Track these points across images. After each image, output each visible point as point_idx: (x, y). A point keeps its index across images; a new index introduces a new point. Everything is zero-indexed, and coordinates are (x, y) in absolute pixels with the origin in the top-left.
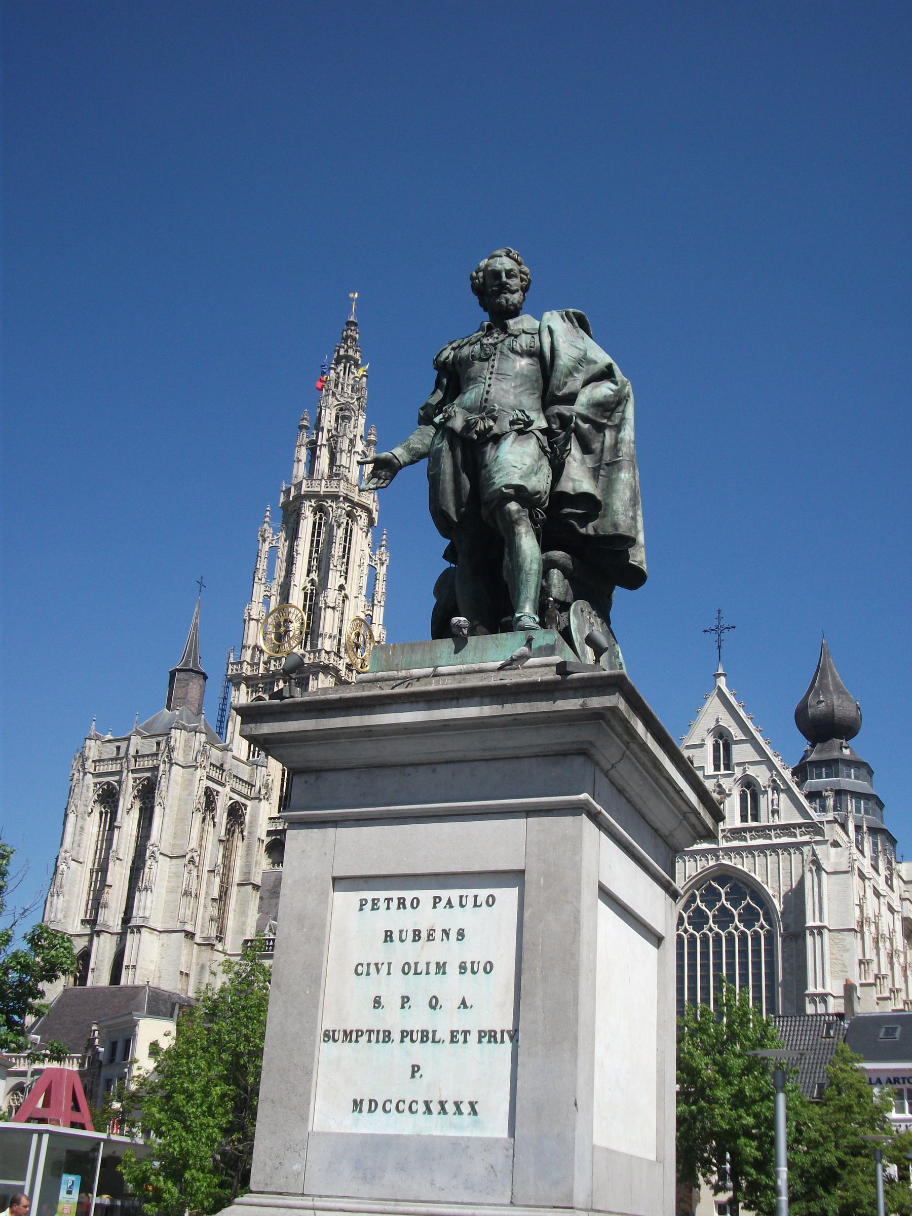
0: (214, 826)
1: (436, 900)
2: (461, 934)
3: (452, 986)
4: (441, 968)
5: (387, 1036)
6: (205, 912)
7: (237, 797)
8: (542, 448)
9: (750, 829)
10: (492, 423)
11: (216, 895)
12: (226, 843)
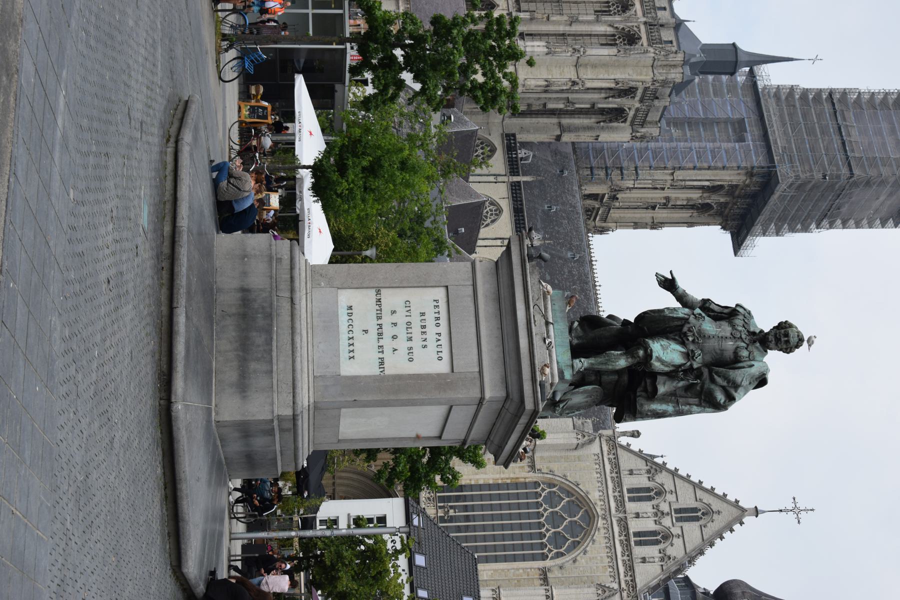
0: (606, 98)
1: (439, 334)
2: (425, 346)
3: (402, 345)
4: (410, 339)
5: (379, 318)
6: (535, 99)
7: (631, 114)
8: (680, 366)
9: (628, 540)
10: (691, 339)
11: (550, 106)
12: (592, 111)
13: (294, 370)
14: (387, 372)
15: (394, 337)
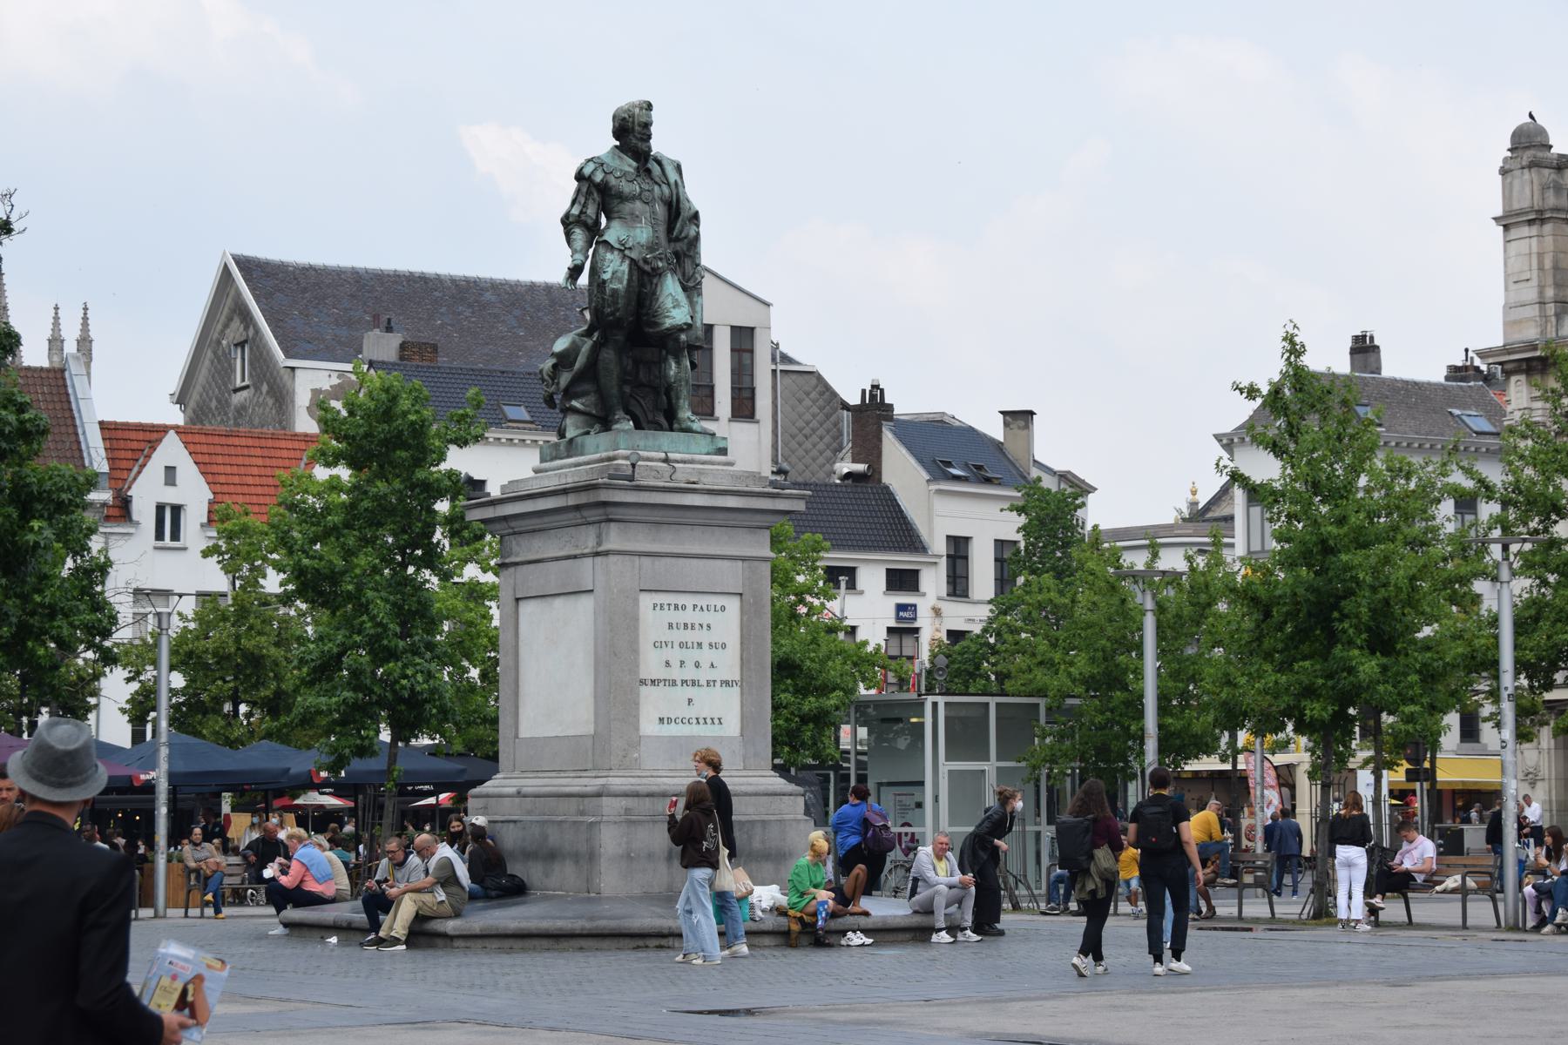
1: (695, 606)
3: (706, 656)
4: (700, 645)
5: (674, 683)
13: (756, 794)
14: (737, 678)
15: (697, 665)
